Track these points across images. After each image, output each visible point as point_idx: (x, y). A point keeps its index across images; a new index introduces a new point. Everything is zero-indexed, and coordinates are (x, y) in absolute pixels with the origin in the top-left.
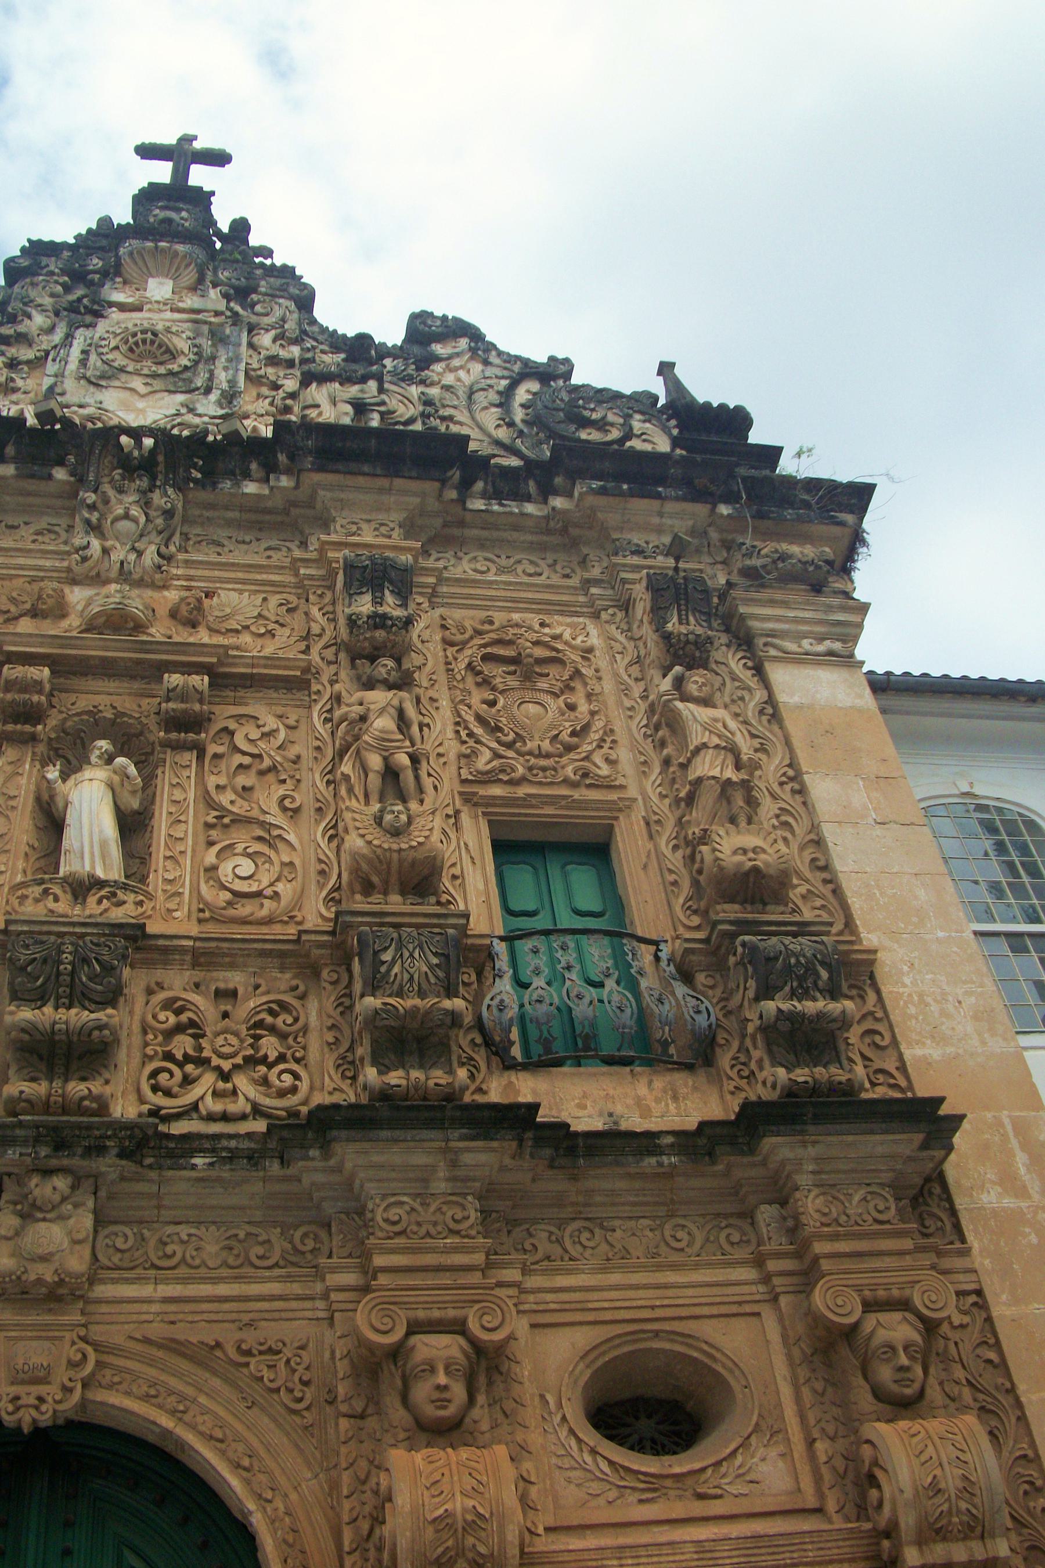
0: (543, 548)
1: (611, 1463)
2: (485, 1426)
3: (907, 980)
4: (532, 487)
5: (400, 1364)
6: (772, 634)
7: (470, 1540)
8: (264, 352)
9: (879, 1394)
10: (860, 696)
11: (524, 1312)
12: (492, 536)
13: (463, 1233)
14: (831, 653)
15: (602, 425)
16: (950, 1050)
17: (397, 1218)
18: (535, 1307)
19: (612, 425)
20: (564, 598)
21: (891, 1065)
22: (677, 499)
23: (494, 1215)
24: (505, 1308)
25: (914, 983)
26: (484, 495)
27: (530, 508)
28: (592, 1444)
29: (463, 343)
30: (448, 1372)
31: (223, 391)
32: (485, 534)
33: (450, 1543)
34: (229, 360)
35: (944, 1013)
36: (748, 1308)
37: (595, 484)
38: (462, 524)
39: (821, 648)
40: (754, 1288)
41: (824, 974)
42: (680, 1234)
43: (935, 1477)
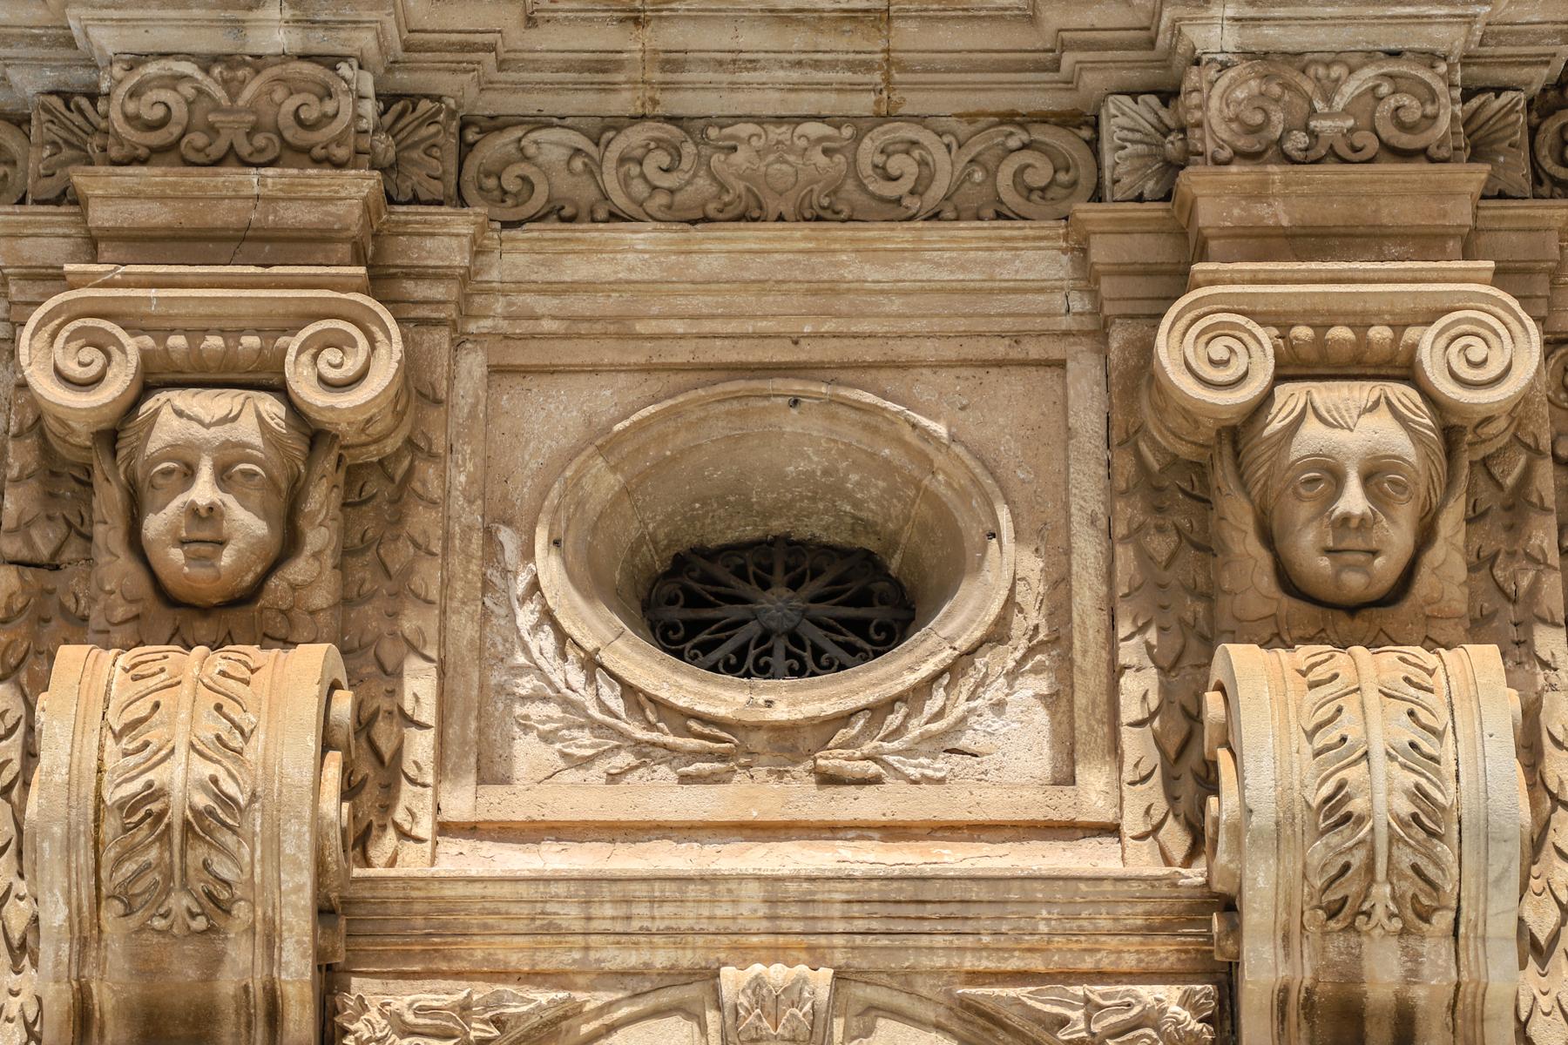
1: (629, 691)
2: (320, 598)
5: (122, 453)
7: (198, 853)
9: (1287, 580)
11: (478, 338)
13: (318, 152)
17: (159, 112)
18: (504, 326)
23: (425, 105)
24: (380, 336)
28: (589, 645)
30: (223, 476)
33: (153, 854)
36: (1034, 350)
40: (1058, 300)
42: (895, 164)
43: (1341, 786)
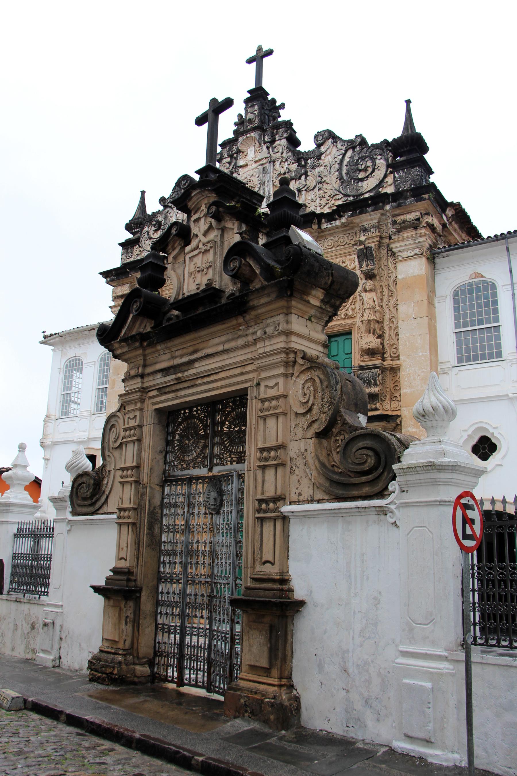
0: (346, 230)
3: (407, 370)
4: (337, 217)
6: (400, 252)
8: (278, 173)
10: (421, 269)
12: (332, 232)
14: (416, 254)
15: (365, 170)
16: (412, 390)
19: (368, 167)
20: (349, 250)
21: (397, 395)
22: (373, 211)
25: (409, 371)
26: (326, 222)
27: (338, 223)
29: (330, 140)
31: (267, 197)
32: (330, 232)
34: (268, 182)
35: (414, 379)
37: (349, 213)
38: (323, 232)
39: (413, 254)
41: (373, 381)
